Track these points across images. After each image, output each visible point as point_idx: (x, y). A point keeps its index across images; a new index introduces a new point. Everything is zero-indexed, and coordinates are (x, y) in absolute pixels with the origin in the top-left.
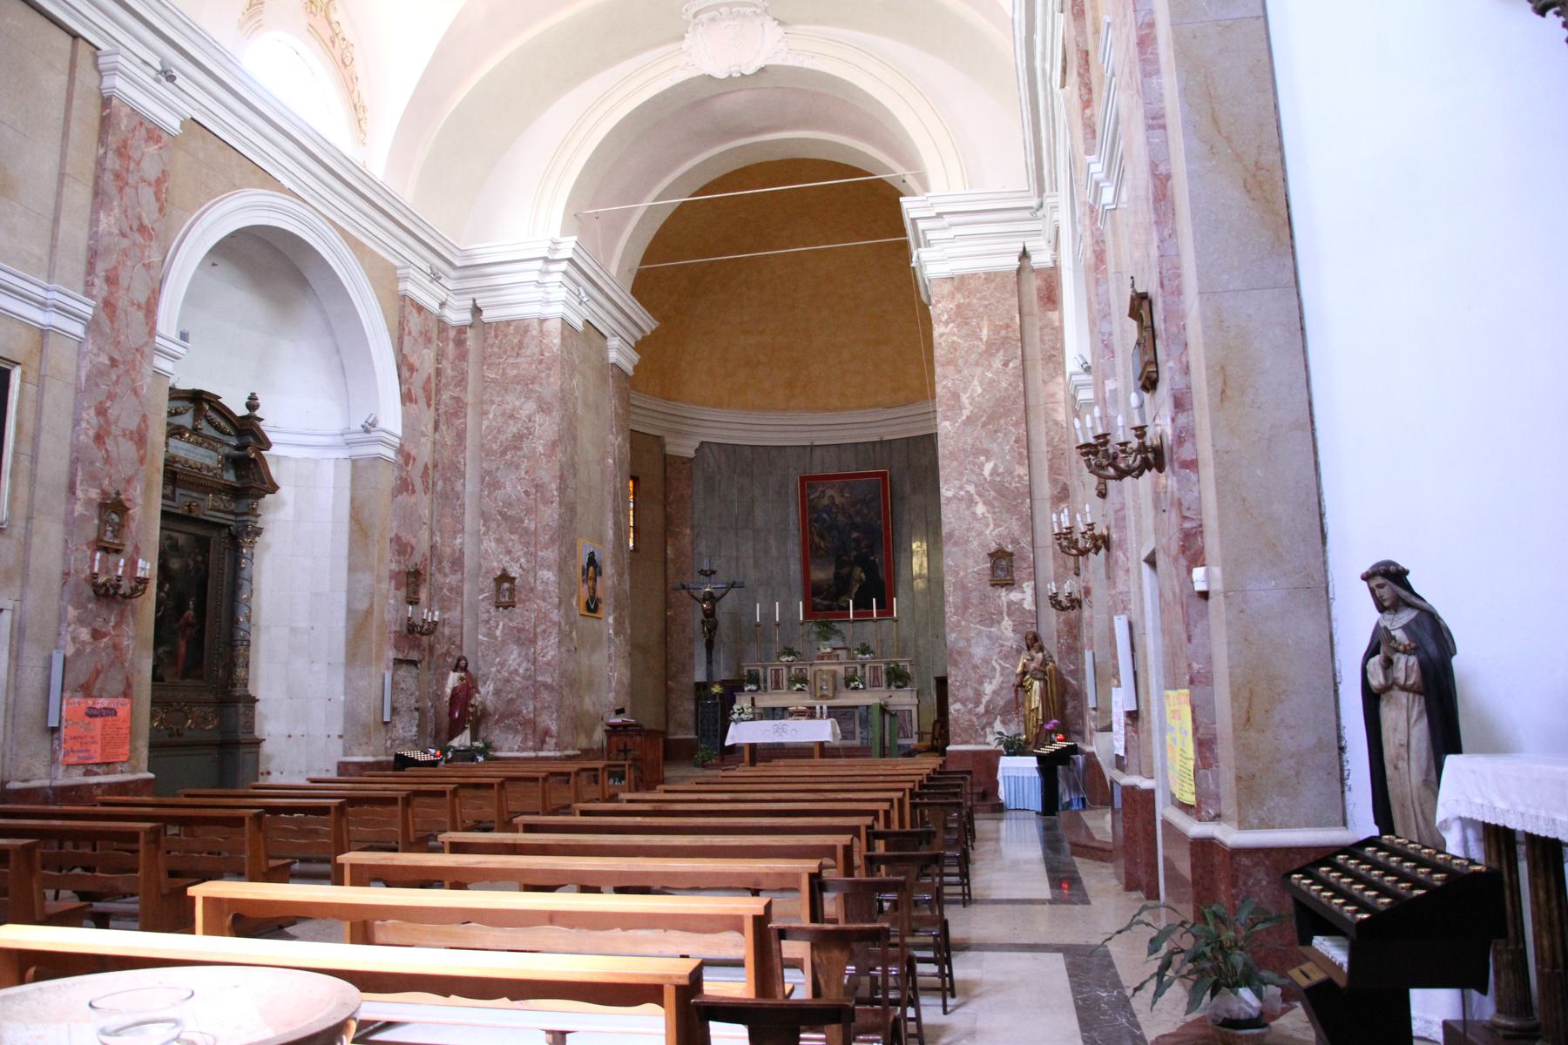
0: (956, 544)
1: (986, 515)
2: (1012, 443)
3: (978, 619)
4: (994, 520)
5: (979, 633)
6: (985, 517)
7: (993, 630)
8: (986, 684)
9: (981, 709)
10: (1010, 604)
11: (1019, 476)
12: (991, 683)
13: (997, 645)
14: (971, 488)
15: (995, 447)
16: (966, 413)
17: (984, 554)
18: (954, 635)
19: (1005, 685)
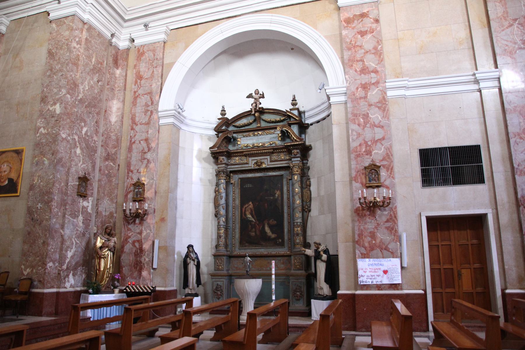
0: (62, 166)
1: (80, 155)
2: (94, 122)
3: (70, 213)
4: (83, 159)
5: (69, 221)
6: (79, 156)
7: (75, 220)
8: (68, 252)
9: (65, 267)
10: (83, 207)
11: (95, 141)
12: (71, 251)
13: (75, 229)
14: (76, 137)
15: (88, 121)
16: (81, 96)
17: (76, 176)
18: (54, 220)
19: (76, 253)
